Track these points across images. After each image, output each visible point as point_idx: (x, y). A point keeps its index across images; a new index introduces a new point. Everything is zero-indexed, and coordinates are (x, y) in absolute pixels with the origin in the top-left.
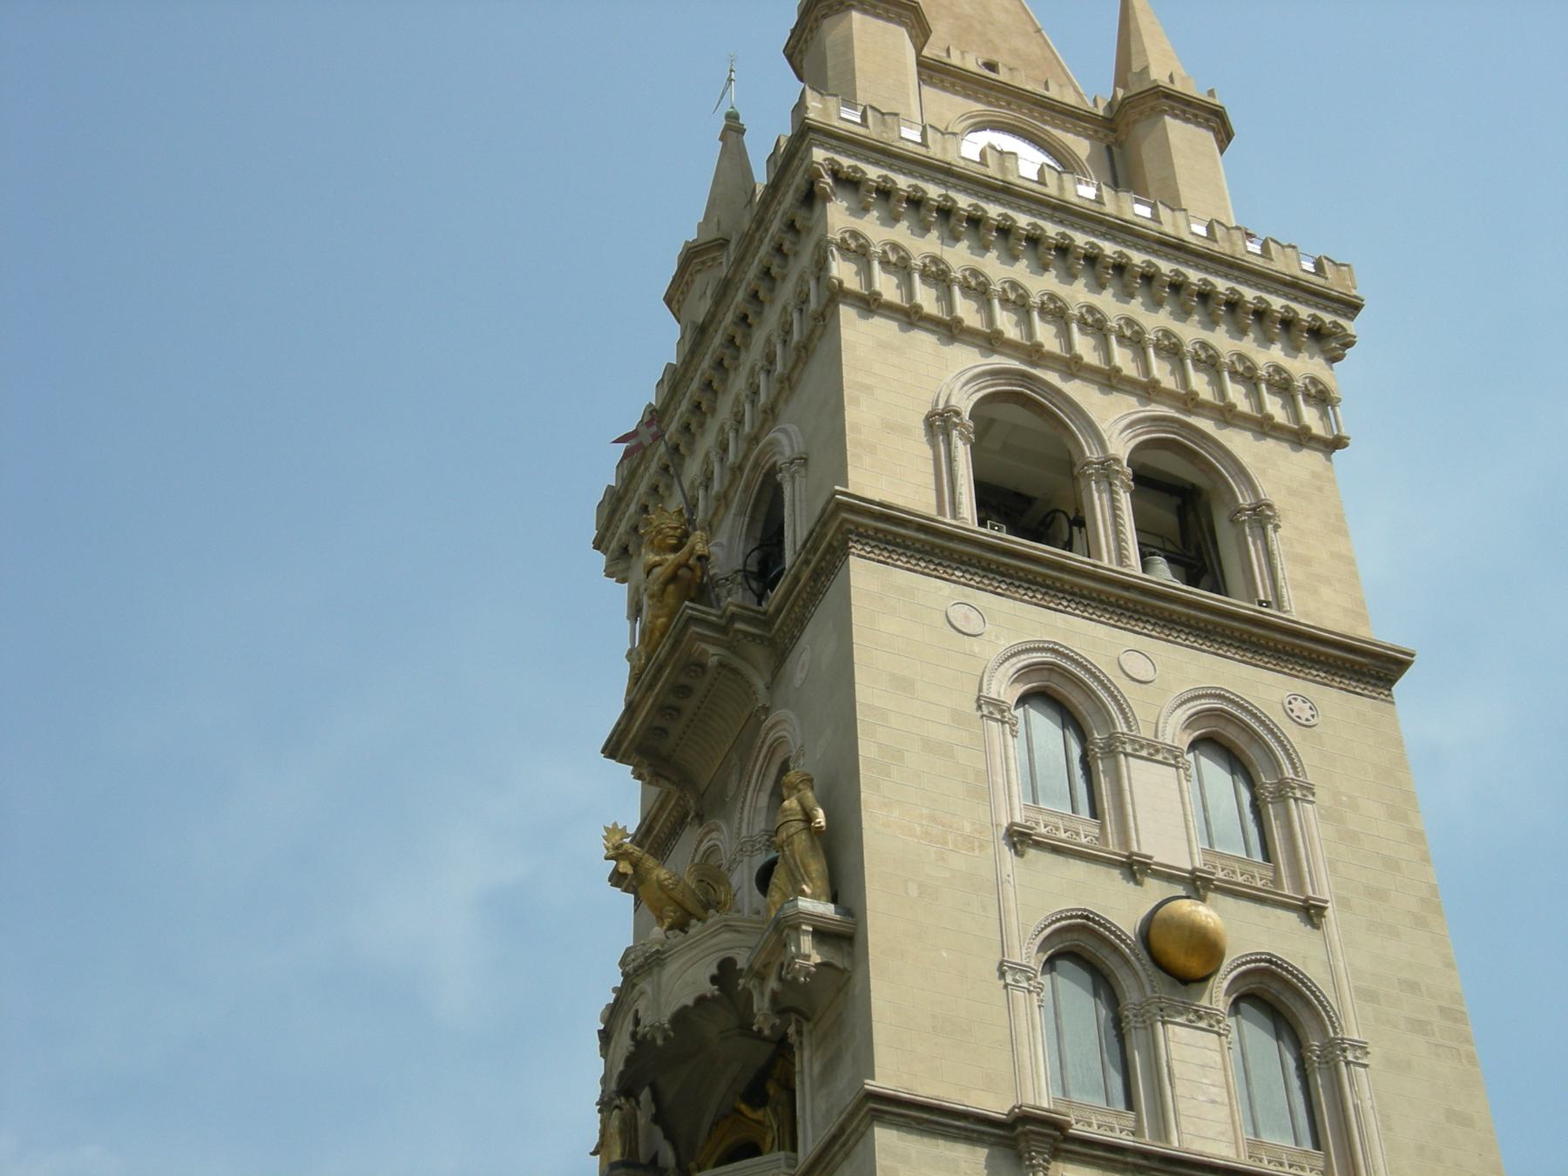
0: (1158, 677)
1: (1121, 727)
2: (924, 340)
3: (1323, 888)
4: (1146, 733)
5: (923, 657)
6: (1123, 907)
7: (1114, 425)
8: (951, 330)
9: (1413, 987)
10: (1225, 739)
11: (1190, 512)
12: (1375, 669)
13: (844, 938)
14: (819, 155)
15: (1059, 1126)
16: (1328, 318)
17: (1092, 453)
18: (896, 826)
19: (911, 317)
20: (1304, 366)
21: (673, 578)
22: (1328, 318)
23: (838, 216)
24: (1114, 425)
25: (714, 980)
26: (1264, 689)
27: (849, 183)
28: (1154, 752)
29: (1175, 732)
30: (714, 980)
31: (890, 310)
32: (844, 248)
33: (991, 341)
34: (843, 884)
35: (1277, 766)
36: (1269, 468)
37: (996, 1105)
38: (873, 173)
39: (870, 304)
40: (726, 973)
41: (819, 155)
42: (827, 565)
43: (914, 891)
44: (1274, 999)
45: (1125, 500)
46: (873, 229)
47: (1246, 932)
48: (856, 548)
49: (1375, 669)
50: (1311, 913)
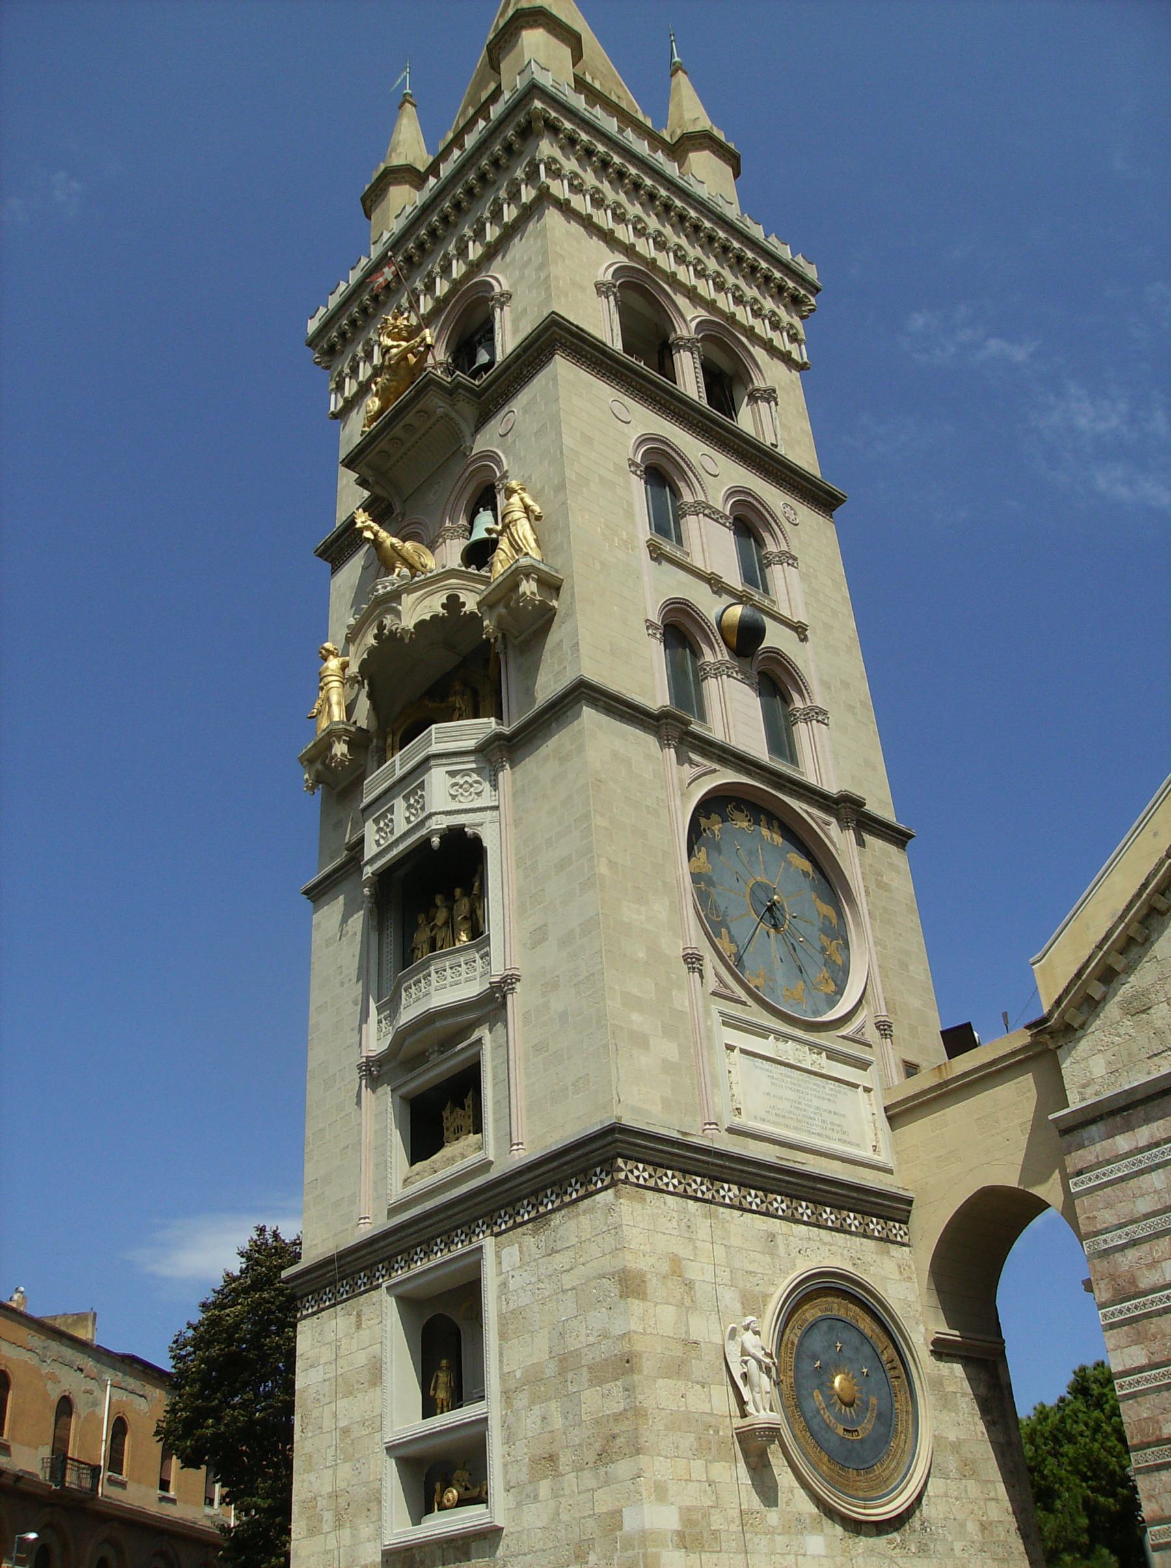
0: (717, 475)
8: (608, 238)
10: (748, 523)
25: (443, 606)
27: (553, 129)
30: (443, 606)
39: (564, 207)
40: (453, 603)
41: (538, 104)
43: (598, 567)
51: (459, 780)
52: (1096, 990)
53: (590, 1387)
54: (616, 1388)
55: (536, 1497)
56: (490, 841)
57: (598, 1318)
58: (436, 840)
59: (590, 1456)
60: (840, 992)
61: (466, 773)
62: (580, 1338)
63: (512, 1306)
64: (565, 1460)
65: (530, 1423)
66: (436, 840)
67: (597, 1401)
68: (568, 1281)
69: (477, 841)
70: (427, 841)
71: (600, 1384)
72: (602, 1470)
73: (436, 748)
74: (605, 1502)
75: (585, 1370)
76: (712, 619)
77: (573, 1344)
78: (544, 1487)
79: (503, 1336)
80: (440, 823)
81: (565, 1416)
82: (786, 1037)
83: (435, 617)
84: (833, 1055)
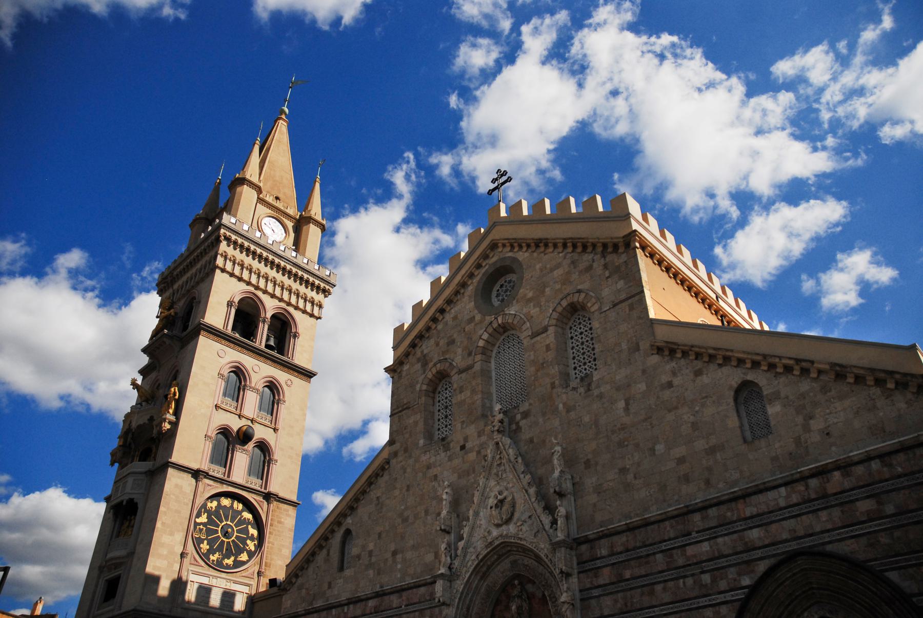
0: (260, 371)
1: (248, 383)
2: (234, 280)
3: (280, 426)
4: (253, 385)
5: (210, 360)
6: (236, 424)
7: (270, 306)
8: (240, 279)
9: (292, 448)
11: (283, 328)
12: (308, 375)
13: (175, 425)
14: (222, 231)
15: (207, 474)
16: (327, 287)
17: (263, 315)
18: (191, 400)
19: (232, 275)
20: (319, 297)
21: (166, 317)
22: (327, 287)
23: (223, 246)
24: (270, 306)
26: (281, 376)
28: (254, 389)
29: (260, 386)
31: (228, 272)
32: (222, 255)
33: (249, 283)
34: (177, 413)
35: (279, 395)
36: (302, 321)
37: (195, 466)
38: (234, 237)
42: (195, 335)
44: (263, 446)
45: (266, 327)
46: (230, 251)
47: (260, 432)
48: (202, 332)
49: (308, 375)
50: (275, 430)
52: (294, 580)
56: (140, 506)
58: (124, 503)
60: (248, 561)
66: (124, 503)
70: (122, 501)
76: (235, 429)
82: (217, 577)
84: (235, 582)
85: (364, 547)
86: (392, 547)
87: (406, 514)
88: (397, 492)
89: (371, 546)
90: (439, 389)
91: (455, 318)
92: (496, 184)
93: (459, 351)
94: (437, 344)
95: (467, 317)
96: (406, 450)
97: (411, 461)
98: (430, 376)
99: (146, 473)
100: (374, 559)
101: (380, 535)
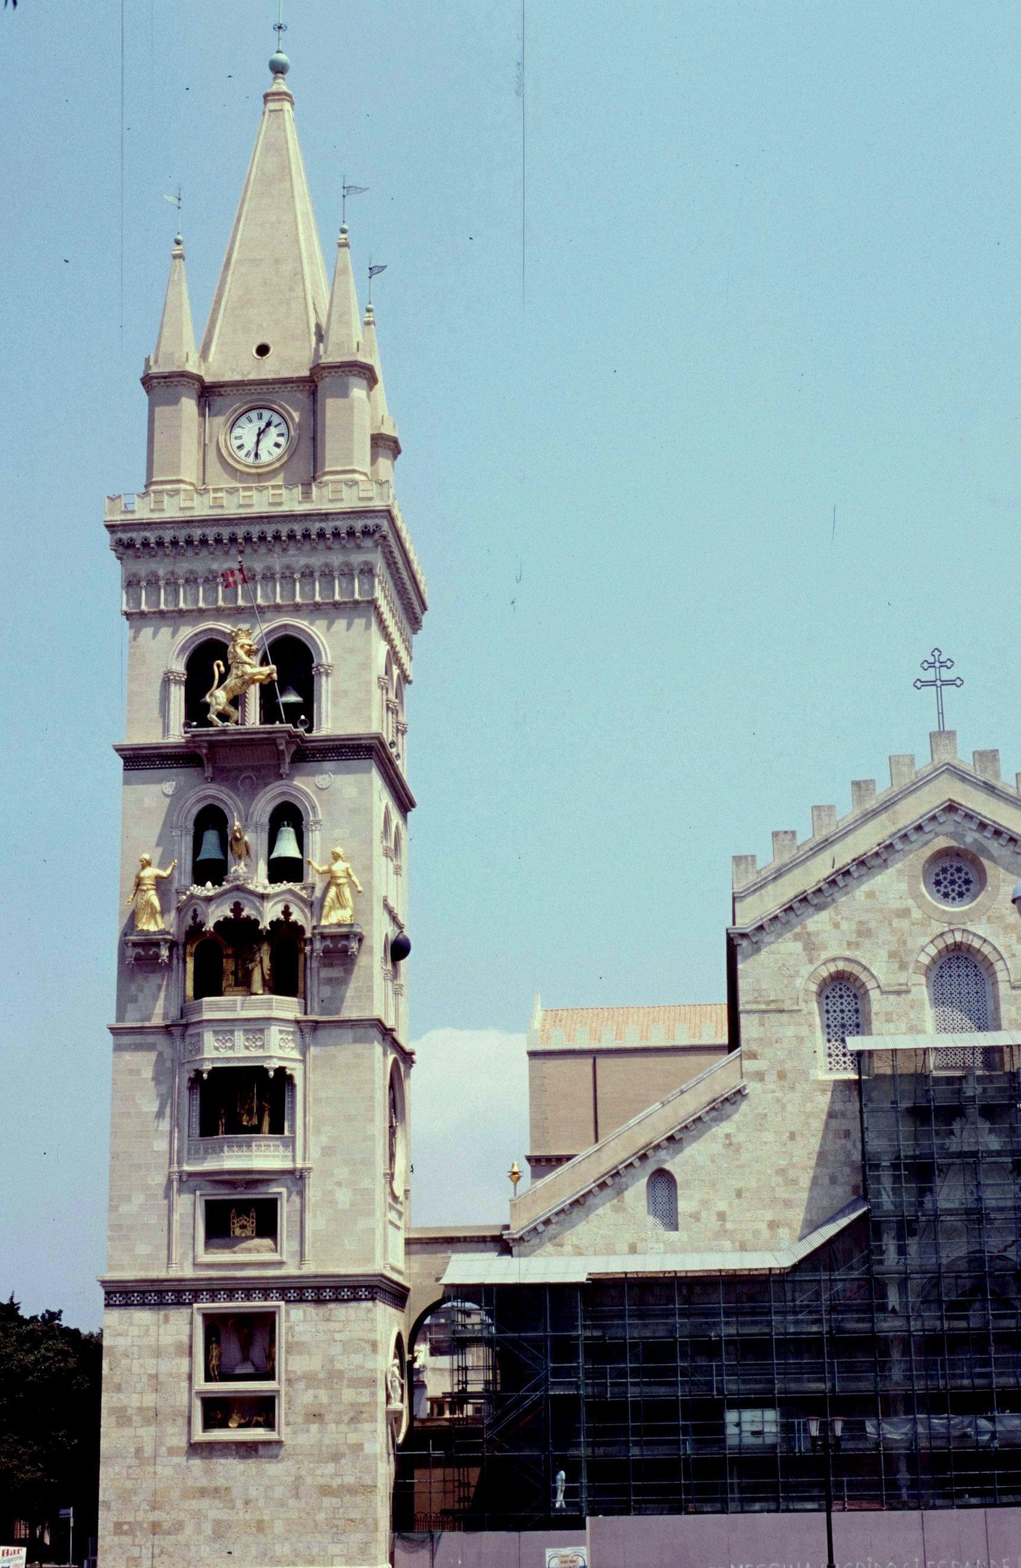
51: (284, 1036)
53: (349, 1386)
54: (366, 1392)
55: (308, 1431)
56: (298, 1081)
57: (357, 1359)
59: (346, 1418)
61: (288, 1033)
62: (343, 1363)
63: (295, 1339)
64: (328, 1417)
65: (306, 1397)
67: (348, 1395)
68: (338, 1337)
69: (291, 1077)
71: (355, 1387)
72: (353, 1426)
73: (276, 1014)
74: (353, 1438)
75: (346, 1381)
77: (338, 1366)
78: (314, 1428)
79: (287, 1352)
80: (276, 1064)
81: (331, 1397)
83: (278, 920)
85: (704, 1203)
86: (769, 1215)
87: (791, 1174)
88: (769, 1136)
89: (722, 1206)
90: (827, 992)
91: (871, 895)
92: (930, 675)
93: (883, 954)
94: (837, 926)
95: (895, 904)
96: (782, 1076)
97: (796, 1096)
98: (824, 973)
99: (297, 1022)
100: (729, 1226)
101: (739, 1194)
